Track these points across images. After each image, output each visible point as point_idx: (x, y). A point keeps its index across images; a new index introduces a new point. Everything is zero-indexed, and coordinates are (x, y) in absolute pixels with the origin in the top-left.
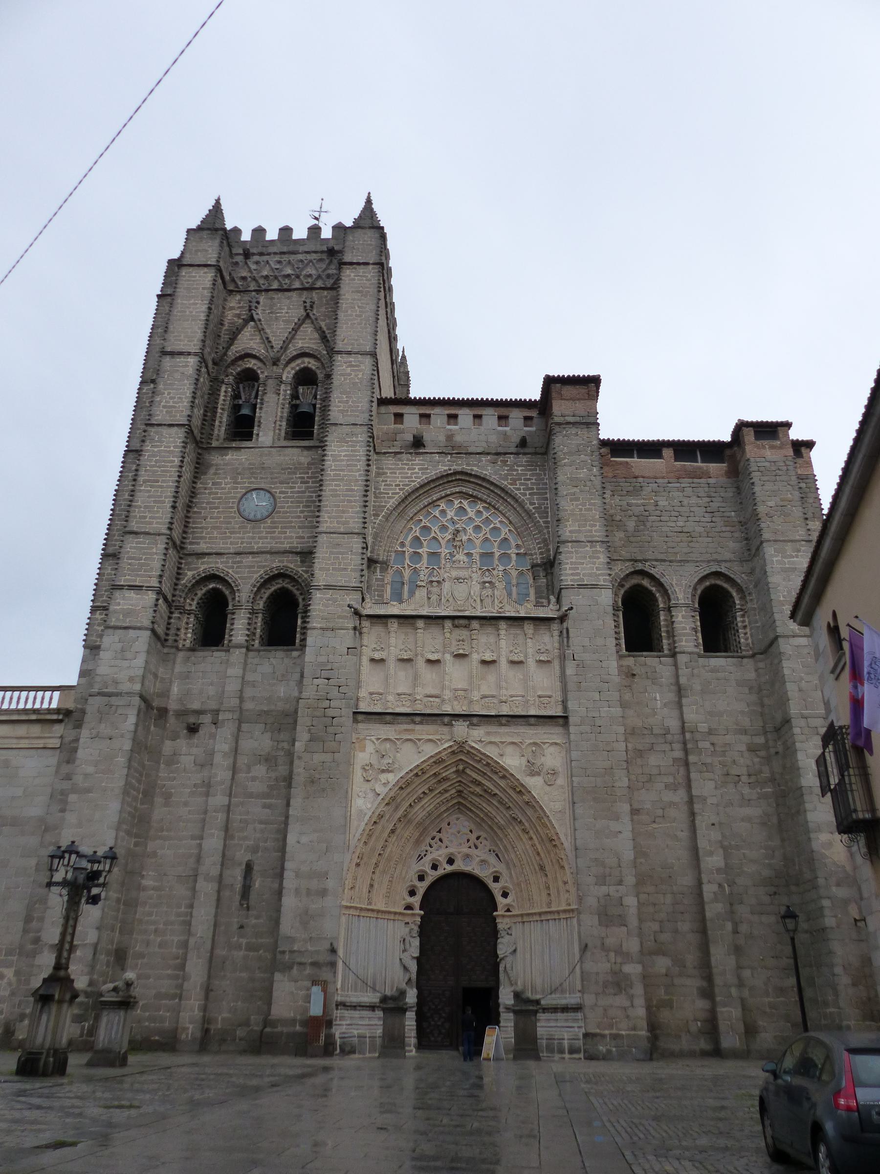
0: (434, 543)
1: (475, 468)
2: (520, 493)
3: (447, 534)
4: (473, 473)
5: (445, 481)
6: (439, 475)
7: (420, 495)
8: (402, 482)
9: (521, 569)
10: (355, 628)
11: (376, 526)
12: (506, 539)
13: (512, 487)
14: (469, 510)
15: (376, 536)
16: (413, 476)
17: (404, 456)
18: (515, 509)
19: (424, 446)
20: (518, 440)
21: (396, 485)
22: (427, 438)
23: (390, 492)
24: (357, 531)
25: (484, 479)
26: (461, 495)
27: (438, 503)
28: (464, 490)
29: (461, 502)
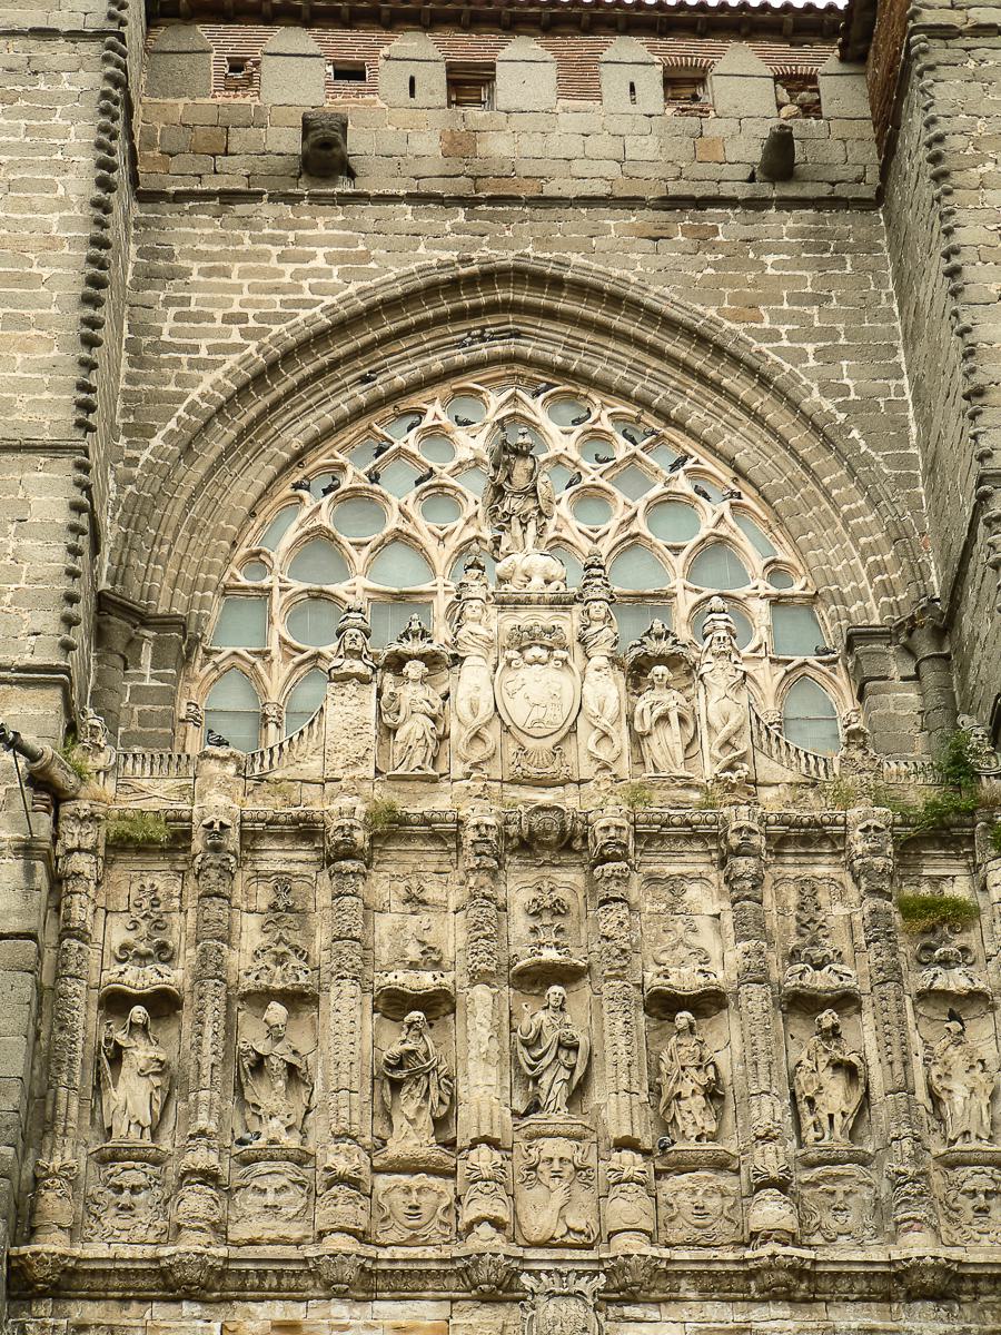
0: (398, 559)
1: (576, 259)
2: (776, 351)
3: (461, 522)
4: (568, 275)
5: (446, 308)
6: (421, 282)
7: (335, 364)
8: (258, 304)
9: (798, 660)
10: (26, 849)
11: (136, 472)
12: (721, 541)
13: (739, 328)
14: (551, 428)
15: (137, 513)
16: (305, 284)
17: (266, 210)
18: (758, 418)
19: (352, 175)
20: (756, 155)
21: (228, 319)
22: (357, 143)
23: (204, 343)
24: (47, 437)
25: (615, 301)
26: (518, 368)
27: (415, 401)
28: (529, 348)
29: (514, 397)
